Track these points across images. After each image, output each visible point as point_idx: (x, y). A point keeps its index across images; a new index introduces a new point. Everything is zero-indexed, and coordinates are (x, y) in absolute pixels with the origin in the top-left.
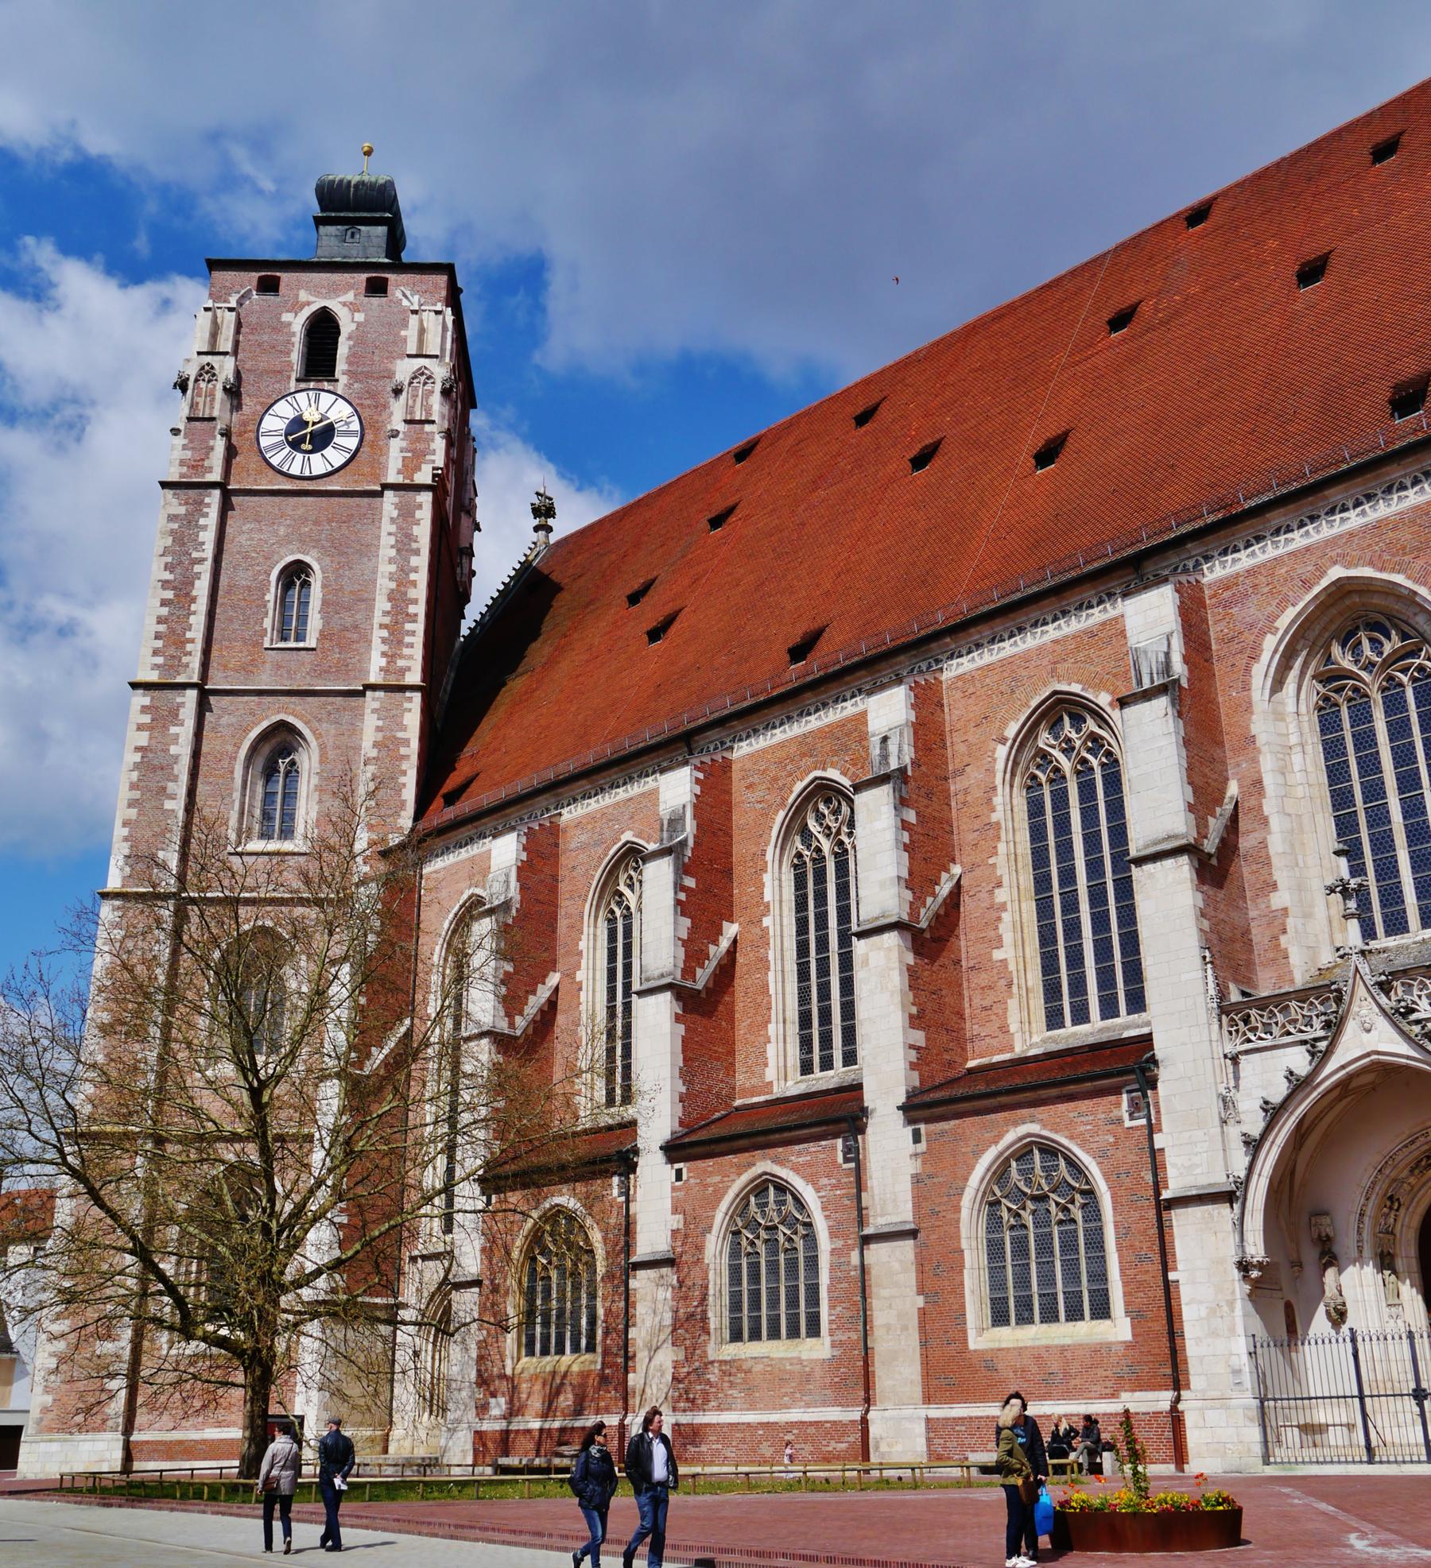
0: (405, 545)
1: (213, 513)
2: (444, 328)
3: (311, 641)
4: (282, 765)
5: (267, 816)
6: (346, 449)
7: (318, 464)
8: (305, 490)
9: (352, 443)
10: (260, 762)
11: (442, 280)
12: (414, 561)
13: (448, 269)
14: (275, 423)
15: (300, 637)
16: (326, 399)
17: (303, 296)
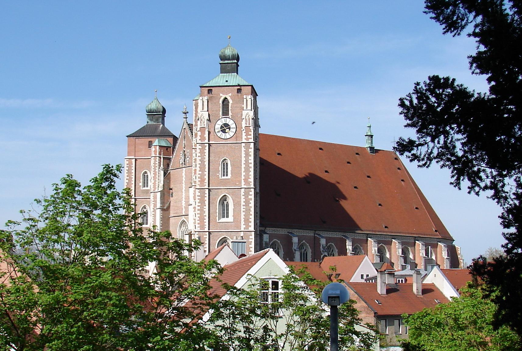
0: (247, 155)
1: (207, 148)
2: (251, 100)
3: (229, 176)
4: (225, 202)
5: (223, 213)
6: (233, 132)
7: (228, 136)
8: (225, 143)
9: (234, 130)
10: (221, 202)
11: (250, 87)
12: (250, 158)
13: (252, 86)
14: (218, 126)
15: (227, 175)
16: (228, 119)
17: (221, 95)
